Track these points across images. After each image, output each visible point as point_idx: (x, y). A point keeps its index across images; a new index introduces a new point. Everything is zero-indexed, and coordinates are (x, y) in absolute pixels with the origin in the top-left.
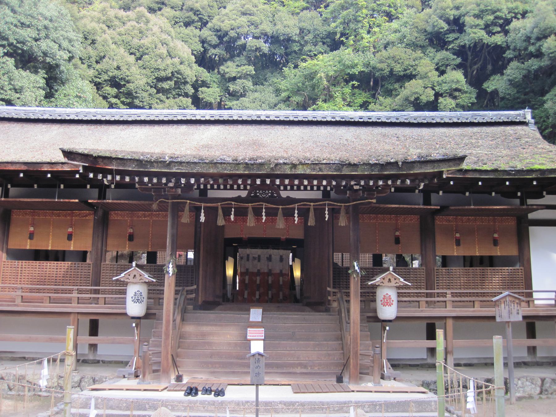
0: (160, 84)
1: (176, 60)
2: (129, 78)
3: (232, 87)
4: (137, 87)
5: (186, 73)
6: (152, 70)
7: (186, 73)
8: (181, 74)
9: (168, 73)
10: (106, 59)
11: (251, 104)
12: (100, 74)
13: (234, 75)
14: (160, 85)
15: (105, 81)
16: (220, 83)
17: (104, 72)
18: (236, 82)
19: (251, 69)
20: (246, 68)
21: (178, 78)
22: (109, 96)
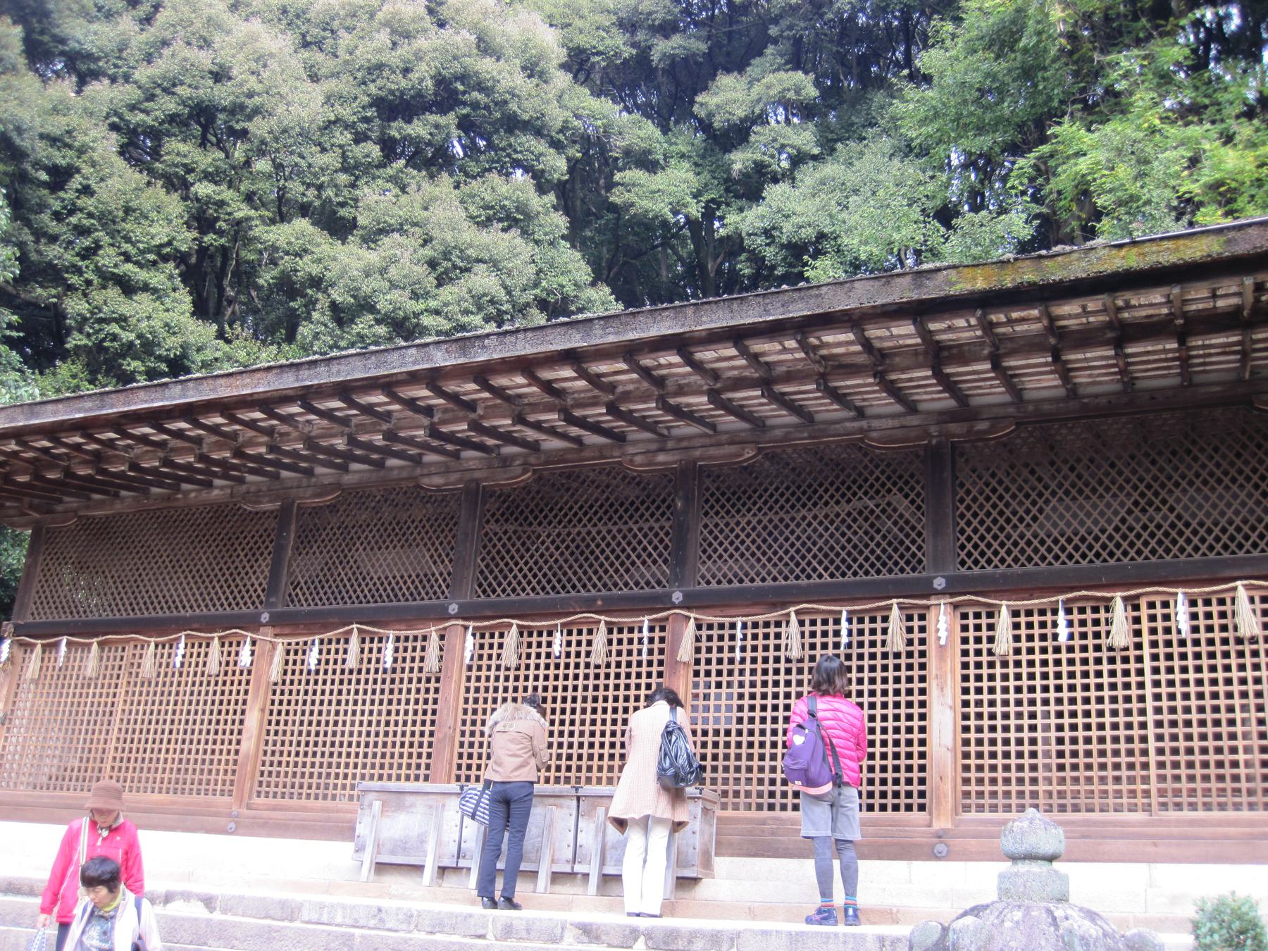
0: (399, 123)
1: (463, 39)
2: (257, 100)
3: (739, 161)
4: (285, 131)
5: (505, 84)
6: (359, 75)
7: (505, 84)
8: (480, 87)
9: (423, 77)
10: (178, 45)
11: (808, 202)
12: (151, 97)
13: (740, 113)
14: (396, 129)
15: (172, 118)
16: (703, 157)
17: (165, 90)
18: (753, 138)
19: (805, 85)
20: (780, 81)
21: (475, 106)
22: (190, 178)
